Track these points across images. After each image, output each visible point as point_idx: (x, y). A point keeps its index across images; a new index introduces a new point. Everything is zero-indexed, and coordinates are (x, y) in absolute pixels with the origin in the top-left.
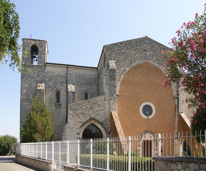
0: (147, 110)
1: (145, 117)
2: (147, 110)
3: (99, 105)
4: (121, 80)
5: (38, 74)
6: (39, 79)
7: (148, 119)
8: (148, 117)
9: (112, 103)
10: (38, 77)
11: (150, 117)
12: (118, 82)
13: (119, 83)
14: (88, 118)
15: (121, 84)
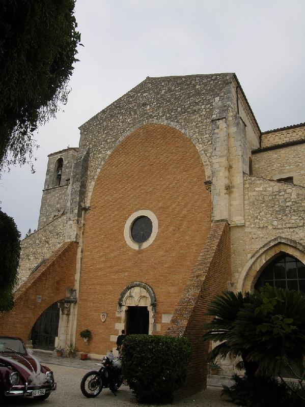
0: (141, 229)
1: (135, 246)
2: (141, 229)
3: (58, 234)
4: (96, 177)
5: (59, 199)
6: (59, 206)
7: (140, 252)
8: (140, 247)
9: (70, 226)
10: (58, 203)
11: (145, 245)
12: (91, 182)
13: (93, 183)
14: (40, 260)
15: (96, 185)
